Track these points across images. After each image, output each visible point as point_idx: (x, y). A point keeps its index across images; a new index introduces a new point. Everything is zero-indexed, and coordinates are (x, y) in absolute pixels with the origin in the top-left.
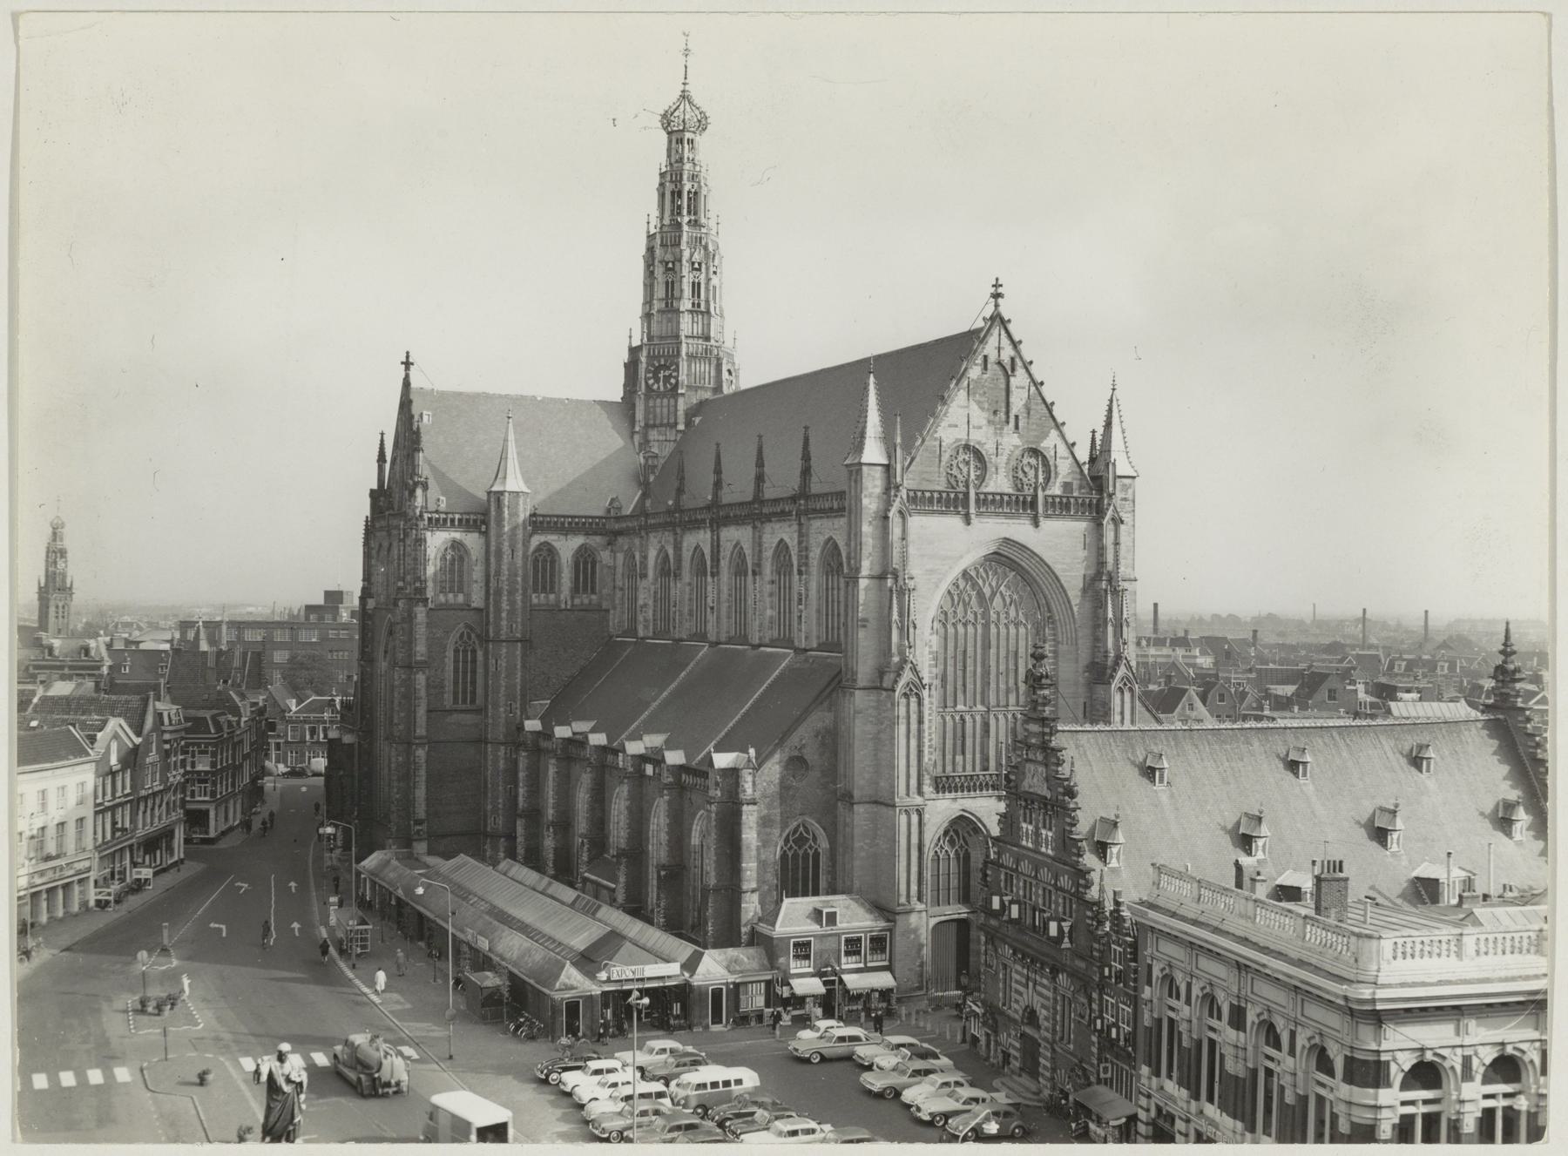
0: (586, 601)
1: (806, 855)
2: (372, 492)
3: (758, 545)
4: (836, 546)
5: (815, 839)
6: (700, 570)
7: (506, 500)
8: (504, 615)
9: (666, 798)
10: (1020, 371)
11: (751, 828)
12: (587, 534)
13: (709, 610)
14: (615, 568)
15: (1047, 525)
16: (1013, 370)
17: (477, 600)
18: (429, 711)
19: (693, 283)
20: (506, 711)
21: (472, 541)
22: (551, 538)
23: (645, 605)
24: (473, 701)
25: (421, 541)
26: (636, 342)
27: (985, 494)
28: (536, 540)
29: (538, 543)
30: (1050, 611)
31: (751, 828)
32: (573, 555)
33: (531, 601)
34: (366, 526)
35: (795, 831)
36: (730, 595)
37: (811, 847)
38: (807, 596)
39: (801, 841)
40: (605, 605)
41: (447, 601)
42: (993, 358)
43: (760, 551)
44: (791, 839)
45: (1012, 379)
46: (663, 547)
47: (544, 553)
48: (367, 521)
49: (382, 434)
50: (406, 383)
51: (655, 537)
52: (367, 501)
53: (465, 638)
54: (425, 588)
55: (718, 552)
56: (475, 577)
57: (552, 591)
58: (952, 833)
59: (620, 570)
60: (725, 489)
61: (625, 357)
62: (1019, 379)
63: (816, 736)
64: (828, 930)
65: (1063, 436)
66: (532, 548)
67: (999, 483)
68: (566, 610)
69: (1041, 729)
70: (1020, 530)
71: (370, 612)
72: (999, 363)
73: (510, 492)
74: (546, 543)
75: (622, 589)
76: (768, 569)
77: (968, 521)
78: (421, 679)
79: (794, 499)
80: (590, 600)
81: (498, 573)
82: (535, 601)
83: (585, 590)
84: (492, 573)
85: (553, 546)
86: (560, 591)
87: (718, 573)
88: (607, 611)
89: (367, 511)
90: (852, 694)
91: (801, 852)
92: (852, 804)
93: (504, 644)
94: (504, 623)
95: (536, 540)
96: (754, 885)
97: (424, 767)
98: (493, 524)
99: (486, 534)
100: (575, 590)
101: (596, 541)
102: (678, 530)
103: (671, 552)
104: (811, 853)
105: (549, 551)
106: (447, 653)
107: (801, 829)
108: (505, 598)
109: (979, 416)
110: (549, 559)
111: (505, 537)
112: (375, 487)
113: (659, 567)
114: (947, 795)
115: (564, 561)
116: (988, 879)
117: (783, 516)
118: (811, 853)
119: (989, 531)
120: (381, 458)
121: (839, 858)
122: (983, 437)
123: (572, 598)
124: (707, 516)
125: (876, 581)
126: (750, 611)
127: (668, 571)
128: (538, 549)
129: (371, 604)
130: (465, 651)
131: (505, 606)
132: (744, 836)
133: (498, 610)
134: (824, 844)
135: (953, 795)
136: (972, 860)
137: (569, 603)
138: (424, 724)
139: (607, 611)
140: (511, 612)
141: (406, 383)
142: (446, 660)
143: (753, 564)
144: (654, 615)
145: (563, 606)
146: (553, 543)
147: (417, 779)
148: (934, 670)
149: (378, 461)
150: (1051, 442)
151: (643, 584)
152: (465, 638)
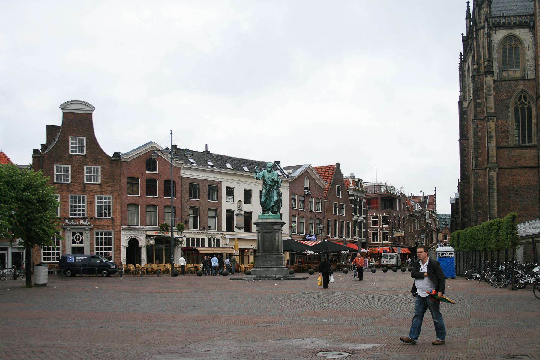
2: (463, 37)
17: (531, 76)
18: (498, 148)
21: (524, 35)
24: (530, 140)
25: (489, 36)
41: (508, 76)
48: (461, 56)
52: (462, 44)
53: (523, 99)
54: (492, 66)
56: (527, 58)
71: (464, 110)
78: (492, 124)
97: (496, 183)
99: (532, 28)
106: (510, 110)
112: (465, 35)
129: (465, 104)
130: (523, 110)
138: (495, 154)
142: (510, 114)
147: (491, 191)
149: (466, 19)
152: (523, 99)
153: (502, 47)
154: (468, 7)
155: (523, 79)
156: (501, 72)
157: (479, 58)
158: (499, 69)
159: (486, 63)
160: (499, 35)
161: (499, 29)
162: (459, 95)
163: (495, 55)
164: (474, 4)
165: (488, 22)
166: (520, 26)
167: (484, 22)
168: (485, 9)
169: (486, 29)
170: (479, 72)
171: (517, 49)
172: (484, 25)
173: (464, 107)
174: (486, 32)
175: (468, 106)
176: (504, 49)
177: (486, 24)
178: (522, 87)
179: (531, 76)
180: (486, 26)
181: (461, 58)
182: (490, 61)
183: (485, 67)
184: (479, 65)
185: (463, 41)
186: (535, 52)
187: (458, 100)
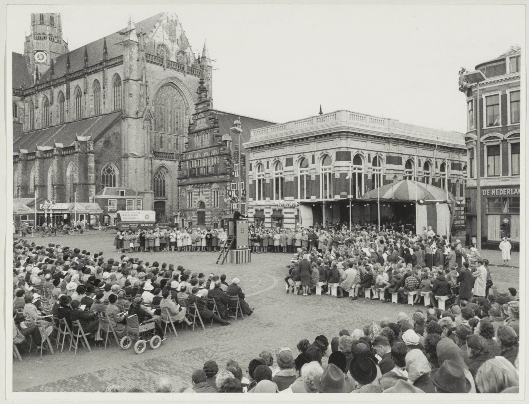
1: (111, 176)
3: (86, 84)
5: (114, 171)
6: (62, 101)
9: (56, 159)
10: (178, 25)
11: (92, 162)
14: (24, 109)
15: (188, 76)
16: (176, 24)
19: (51, 17)
23: (38, 118)
26: (28, 35)
27: (169, 61)
30: (188, 105)
31: (92, 162)
35: (107, 167)
36: (74, 105)
37: (112, 173)
39: (109, 171)
40: (21, 122)
42: (170, 19)
43: (87, 86)
44: (106, 170)
45: (176, 27)
46: (46, 96)
51: (42, 93)
55: (69, 90)
58: (159, 173)
59: (26, 109)
60: (72, 67)
61: (24, 40)
62: (178, 28)
63: (114, 135)
65: (191, 49)
67: (173, 59)
70: (180, 75)
72: (172, 20)
75: (27, 116)
76: (91, 91)
77: (164, 70)
79: (101, 64)
87: (69, 98)
88: (22, 124)
91: (109, 175)
92: (128, 157)
96: (93, 182)
102: (52, 88)
103: (49, 97)
104: (113, 175)
107: (109, 167)
109: (167, 37)
113: (44, 104)
114: (158, 158)
116: (182, 167)
117: (96, 71)
118: (113, 175)
119: (171, 73)
121: (123, 178)
122: (168, 43)
124: (64, 80)
127: (48, 104)
132: (89, 164)
134: (117, 173)
135: (160, 159)
136: (166, 182)
139: (22, 124)
144: (42, 121)
150: (187, 50)
151: (36, 111)
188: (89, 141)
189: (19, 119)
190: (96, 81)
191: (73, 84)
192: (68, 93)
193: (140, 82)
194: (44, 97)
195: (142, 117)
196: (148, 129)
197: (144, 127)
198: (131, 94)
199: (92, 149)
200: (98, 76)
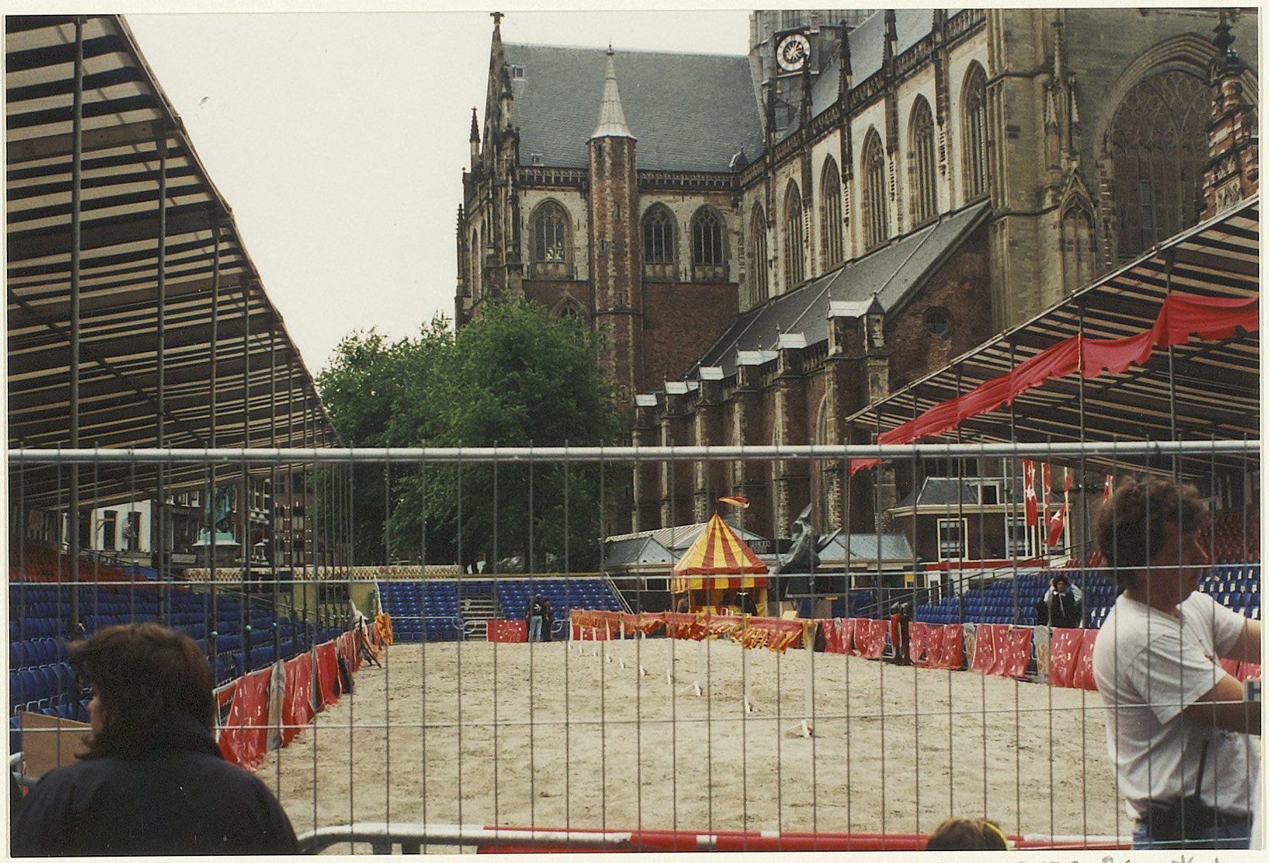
0: (710, 274)
2: (464, 174)
4: (981, 69)
7: (607, 145)
8: (611, 282)
9: (785, 390)
12: (707, 195)
13: (844, 224)
17: (582, 276)
20: (618, 396)
21: (572, 202)
22: (666, 199)
23: (776, 258)
25: (515, 200)
28: (646, 202)
29: (649, 204)
32: (692, 220)
33: (644, 271)
34: (460, 219)
38: (950, 146)
41: (546, 273)
47: (658, 216)
48: (460, 210)
49: (474, 110)
50: (497, 37)
56: (576, 244)
57: (670, 262)
64: (989, 509)
66: (642, 212)
68: (686, 283)
69: (1230, 130)
73: (612, 138)
74: (659, 203)
79: (928, 39)
80: (715, 274)
81: (602, 234)
82: (649, 273)
83: (708, 260)
84: (596, 233)
85: (666, 207)
86: (678, 263)
87: (851, 176)
88: (737, 285)
89: (460, 199)
90: (1003, 223)
93: (613, 317)
94: (611, 292)
95: (646, 202)
98: (594, 178)
99: (585, 191)
100: (696, 260)
101: (723, 204)
105: (661, 216)
108: (611, 262)
110: (663, 223)
111: (608, 190)
112: (469, 171)
115: (681, 224)
120: (474, 137)
123: (693, 270)
125: (1026, 81)
126: (888, 197)
128: (651, 210)
129: (468, 303)
131: (611, 271)
133: (604, 277)
137: (689, 274)
140: (619, 280)
141: (497, 37)
143: (888, 140)
145: (682, 278)
146: (667, 204)
148: (1110, 204)
149: (471, 141)
153: (535, 219)
154: (474, 117)
155: (570, 279)
156: (534, 265)
157: (498, 237)
158: (530, 258)
159: (510, 249)
160: (531, 200)
161: (531, 189)
162: (456, 284)
163: (525, 235)
164: (486, 120)
165: (514, 175)
166: (563, 184)
167: (507, 175)
168: (508, 152)
169: (510, 188)
170: (498, 263)
171: (561, 226)
172: (507, 180)
173: (465, 308)
174: (510, 193)
175: (472, 308)
176: (539, 224)
177: (510, 178)
178: (567, 294)
179: (582, 276)
180: (511, 182)
181: (460, 215)
182: (517, 246)
183: (508, 255)
184: (498, 250)
185: (464, 181)
186: (589, 234)
187: (455, 295)
188: (868, 314)
189: (728, 269)
190: (921, 101)
191: (859, 126)
192: (847, 158)
193: (1043, 78)
194: (789, 186)
195: (1055, 207)
196: (1078, 249)
197: (1062, 241)
198: (1018, 129)
199: (879, 343)
200: (925, 85)
